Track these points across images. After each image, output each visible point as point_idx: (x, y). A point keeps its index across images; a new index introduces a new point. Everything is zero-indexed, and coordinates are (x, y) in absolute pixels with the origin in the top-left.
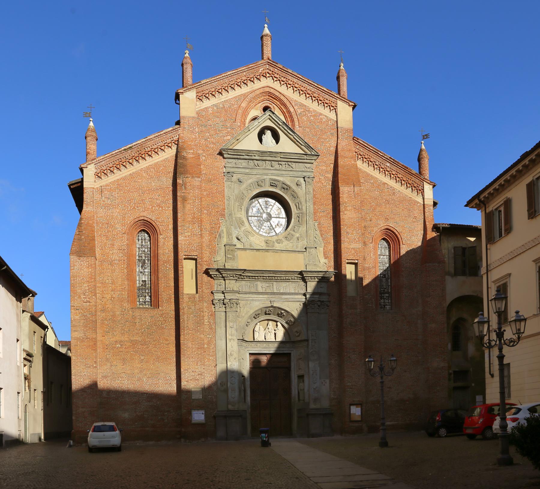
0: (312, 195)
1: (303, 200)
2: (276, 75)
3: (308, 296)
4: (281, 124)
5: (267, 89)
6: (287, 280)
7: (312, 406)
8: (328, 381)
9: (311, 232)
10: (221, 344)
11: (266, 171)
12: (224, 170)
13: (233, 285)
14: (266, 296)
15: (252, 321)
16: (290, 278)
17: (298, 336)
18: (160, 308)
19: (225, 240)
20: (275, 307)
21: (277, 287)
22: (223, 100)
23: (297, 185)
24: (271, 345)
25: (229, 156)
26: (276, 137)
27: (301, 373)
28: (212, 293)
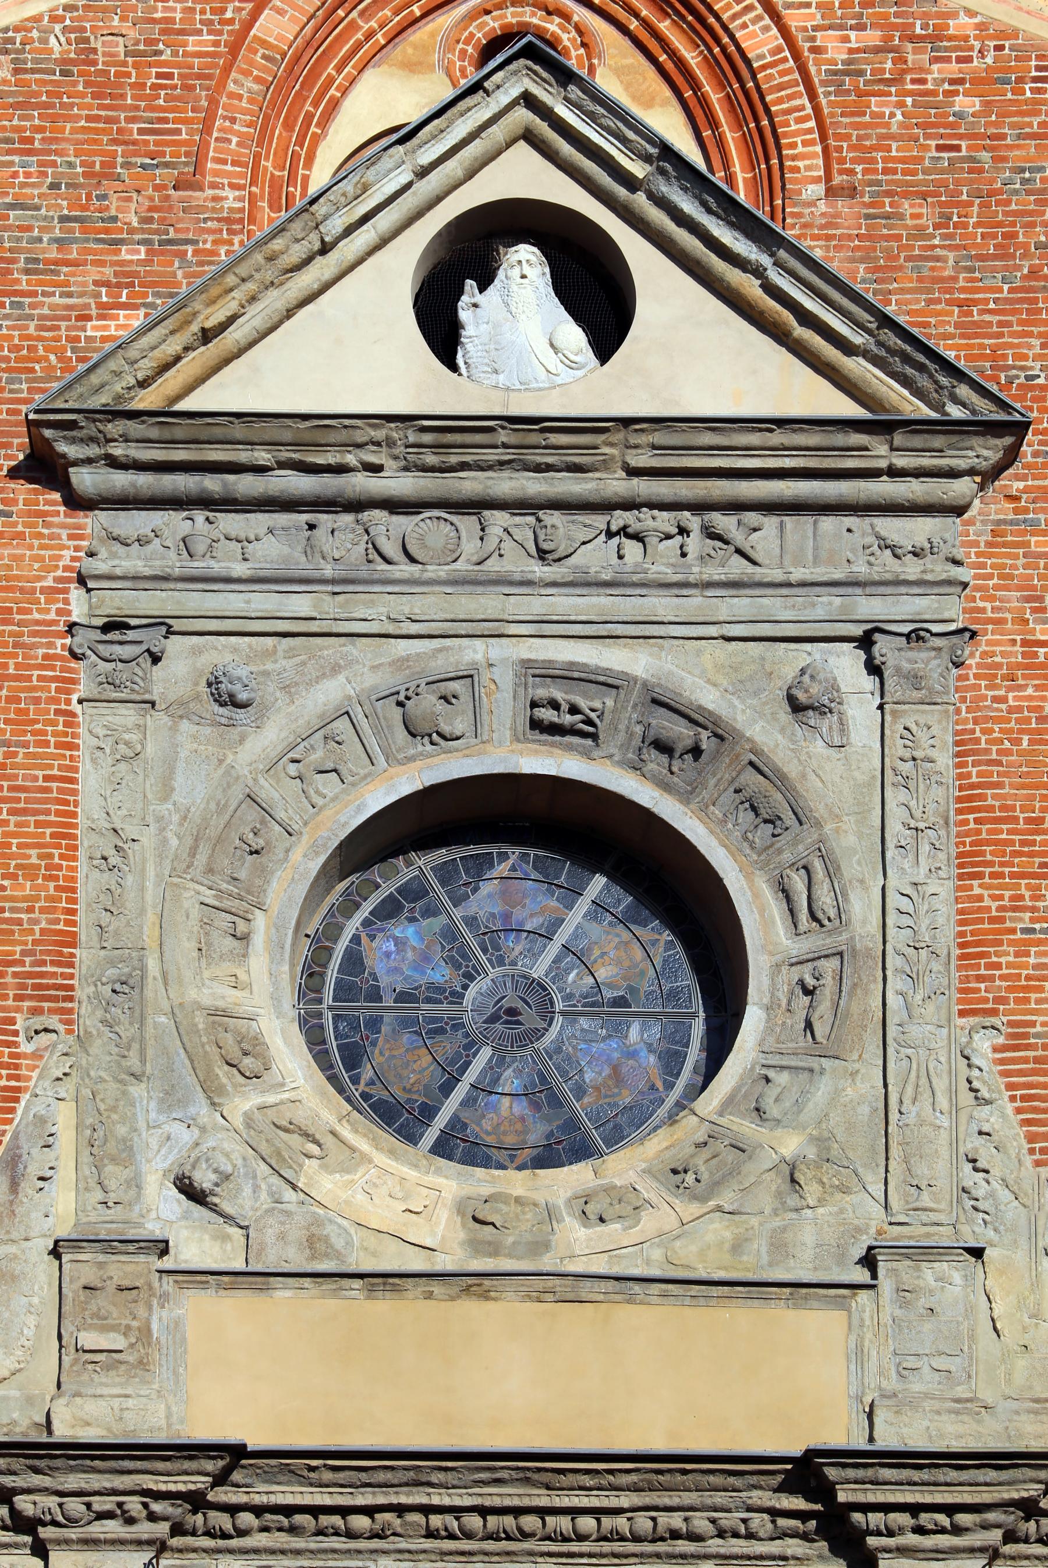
0: (938, 797)
1: (852, 843)
4: (638, 169)
9: (933, 1124)
11: (489, 603)
12: (78, 605)
16: (701, 1523)
19: (61, 1208)
23: (797, 707)
25: (121, 480)
26: (601, 303)
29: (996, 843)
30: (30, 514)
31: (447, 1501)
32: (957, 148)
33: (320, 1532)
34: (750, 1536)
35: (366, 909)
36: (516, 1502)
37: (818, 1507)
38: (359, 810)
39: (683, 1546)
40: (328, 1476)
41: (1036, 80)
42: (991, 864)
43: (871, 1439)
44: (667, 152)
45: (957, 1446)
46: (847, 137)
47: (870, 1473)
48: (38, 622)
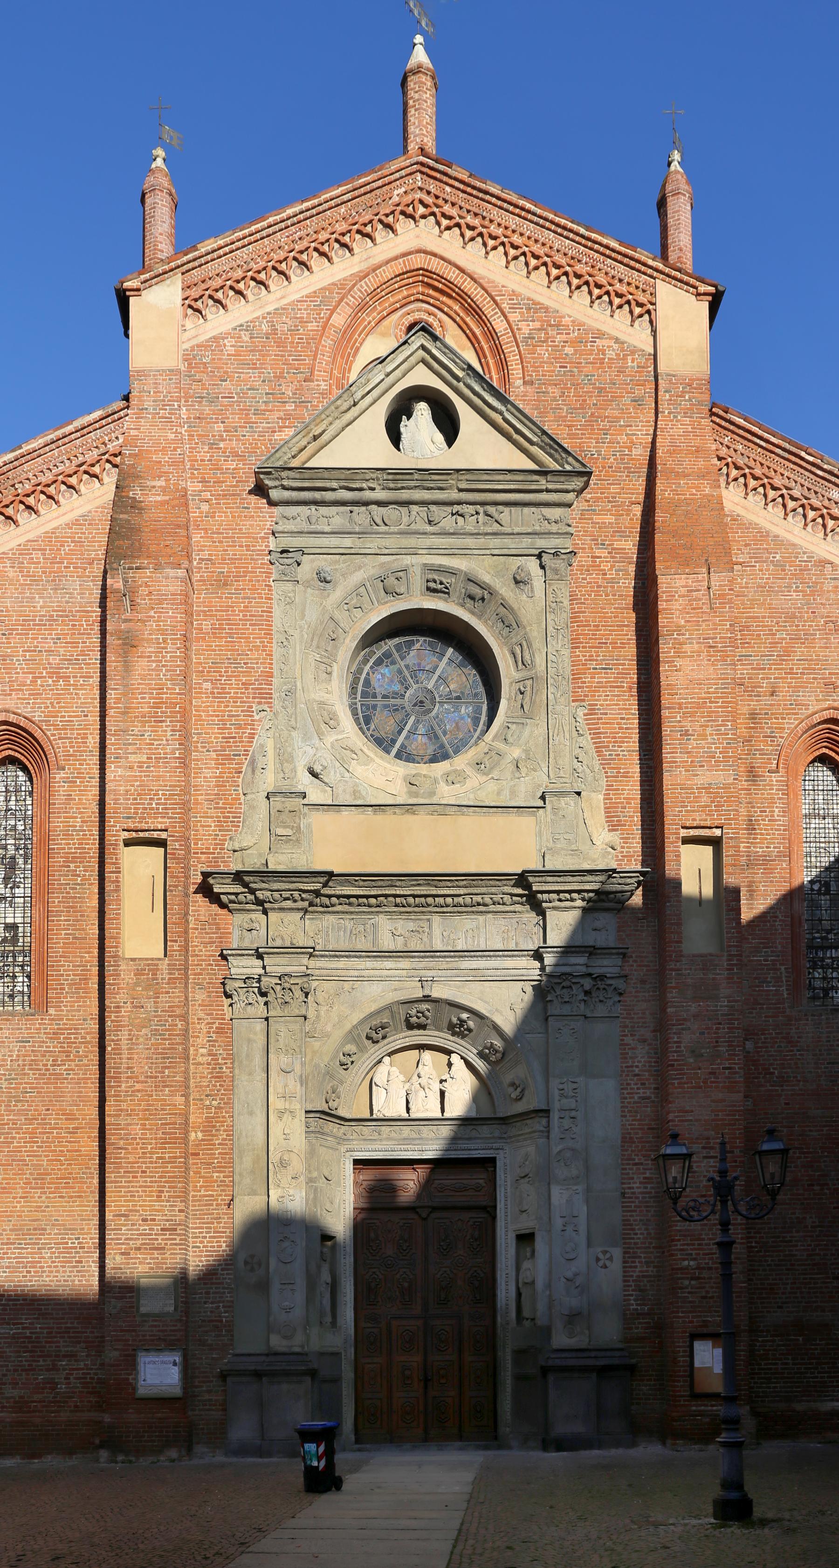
0: (564, 617)
1: (535, 633)
2: (447, 209)
3: (549, 959)
4: (460, 374)
5: (418, 261)
6: (477, 908)
7: (561, 1339)
8: (617, 1253)
9: (563, 742)
10: (249, 1127)
11: (411, 541)
12: (272, 544)
13: (292, 928)
14: (405, 963)
15: (362, 1049)
16: (487, 899)
17: (519, 1099)
18: (52, 1011)
19: (269, 780)
20: (436, 1001)
21: (441, 931)
22: (270, 308)
23: (517, 582)
24: (426, 1131)
25: (287, 495)
26: (448, 424)
27: (526, 1224)
28: (224, 957)
29: (584, 634)
30: (256, 508)
31: (402, 893)
32: (566, 367)
33: (359, 905)
34: (504, 904)
35: (370, 664)
36: (425, 893)
37: (526, 892)
38: (368, 623)
39: (482, 908)
40: (361, 883)
41: (591, 342)
42: (582, 643)
43: (544, 866)
44: (470, 367)
45: (572, 868)
46: (530, 362)
47: (544, 878)
48: (259, 550)
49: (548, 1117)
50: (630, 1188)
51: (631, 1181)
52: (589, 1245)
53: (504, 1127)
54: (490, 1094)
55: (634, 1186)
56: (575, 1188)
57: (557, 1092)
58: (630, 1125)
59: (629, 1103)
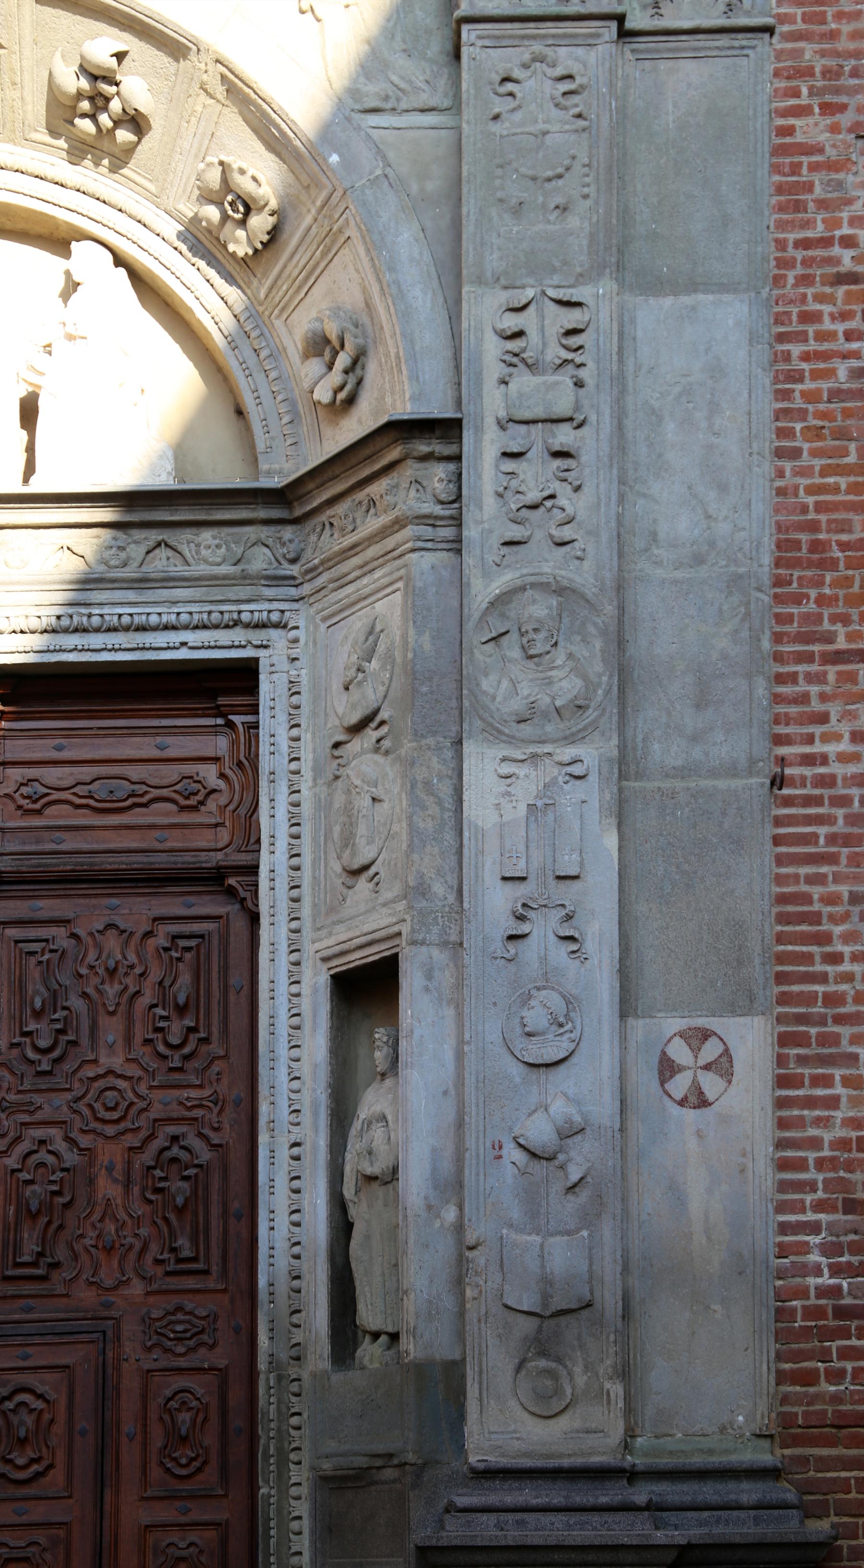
7: (502, 1425)
8: (751, 1039)
27: (366, 921)
49: (457, 458)
50: (809, 760)
51: (817, 730)
52: (627, 1006)
53: (288, 533)
54: (240, 412)
55: (831, 749)
56: (567, 753)
57: (493, 349)
58: (811, 490)
59: (811, 397)
